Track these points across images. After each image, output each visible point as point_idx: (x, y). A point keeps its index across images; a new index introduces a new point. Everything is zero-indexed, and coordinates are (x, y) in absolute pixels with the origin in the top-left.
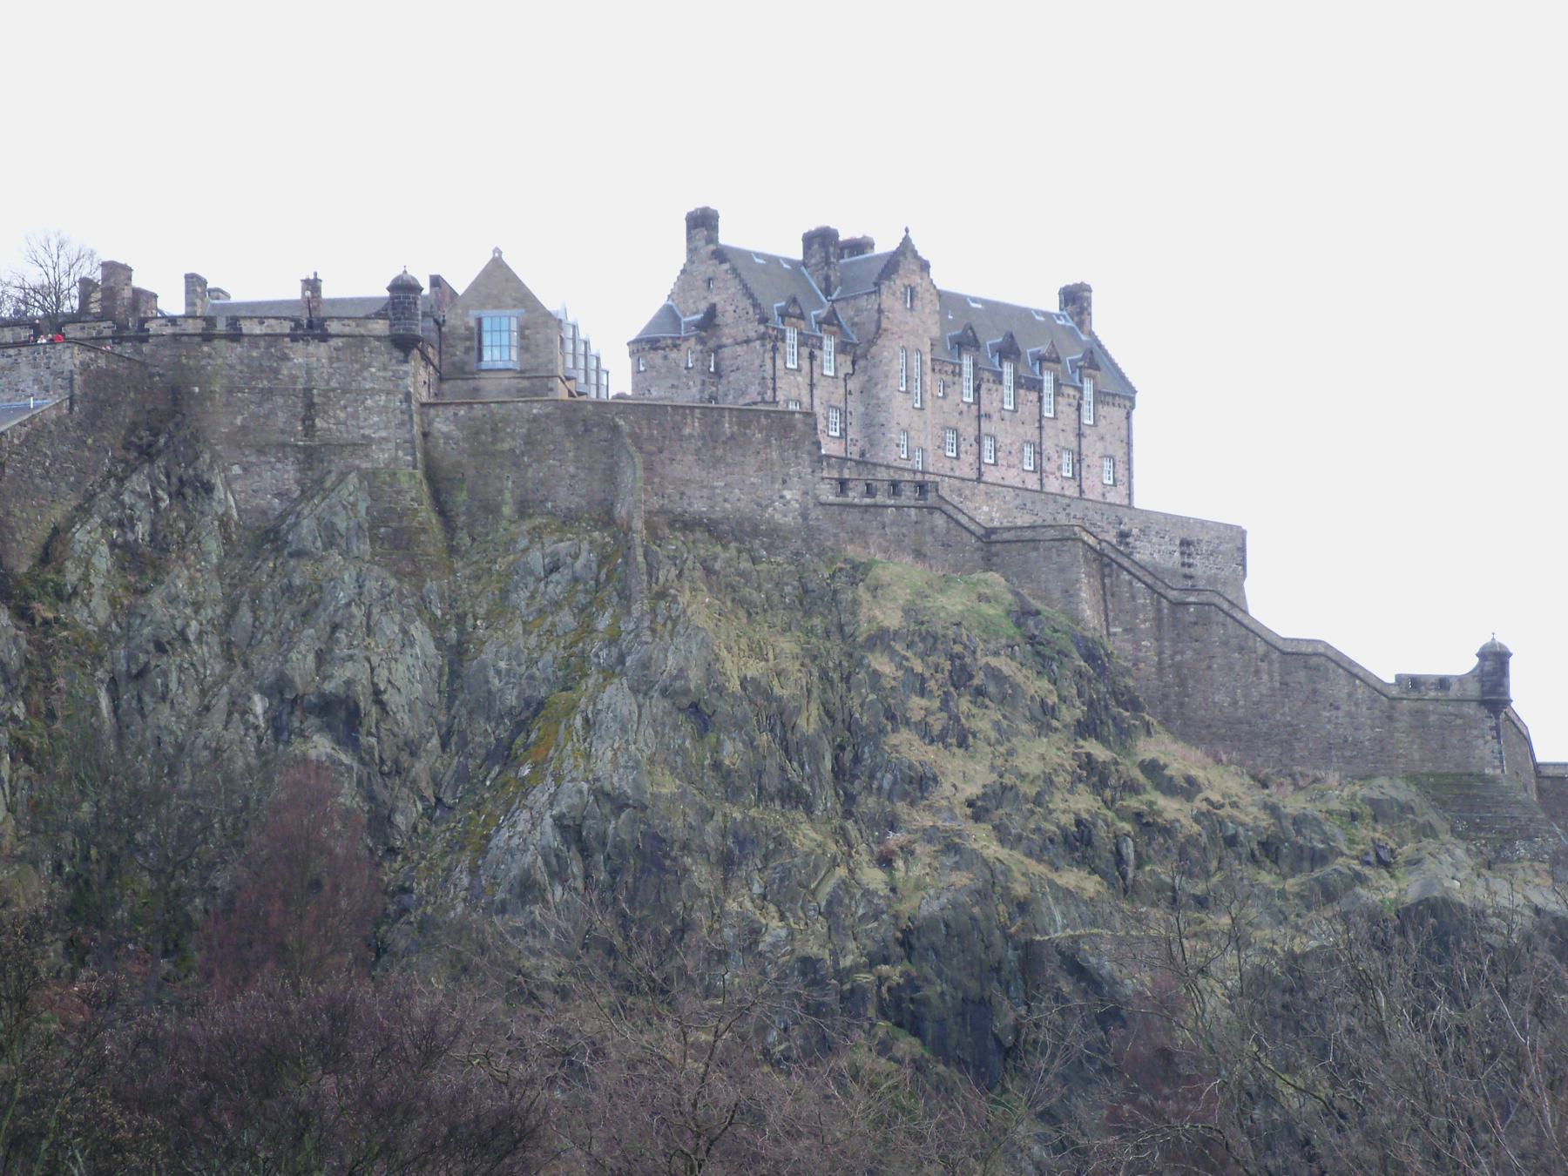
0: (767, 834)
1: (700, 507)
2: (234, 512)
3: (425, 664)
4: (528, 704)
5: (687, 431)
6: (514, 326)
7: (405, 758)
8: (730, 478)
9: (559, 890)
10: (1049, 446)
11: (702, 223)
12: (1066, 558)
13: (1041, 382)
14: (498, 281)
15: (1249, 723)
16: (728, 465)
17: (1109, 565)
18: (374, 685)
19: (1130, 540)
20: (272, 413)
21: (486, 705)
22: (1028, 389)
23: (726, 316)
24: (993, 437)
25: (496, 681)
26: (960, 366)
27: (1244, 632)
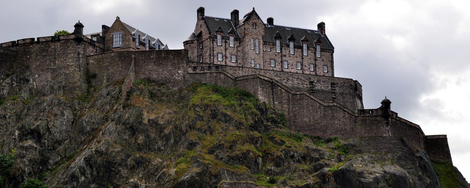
0: (147, 161)
1: (155, 76)
2: (35, 87)
3: (67, 121)
4: (93, 130)
5: (152, 57)
6: (121, 36)
7: (56, 145)
8: (163, 69)
9: (83, 178)
10: (305, 63)
11: (201, 11)
12: (255, 83)
13: (303, 47)
14: (119, 24)
15: (314, 126)
16: (163, 65)
17: (275, 85)
18: (48, 126)
19: (314, 84)
20: (46, 61)
21: (82, 131)
22: (298, 48)
23: (203, 34)
24: (287, 61)
25: (85, 124)
26: (275, 43)
27: (313, 101)
